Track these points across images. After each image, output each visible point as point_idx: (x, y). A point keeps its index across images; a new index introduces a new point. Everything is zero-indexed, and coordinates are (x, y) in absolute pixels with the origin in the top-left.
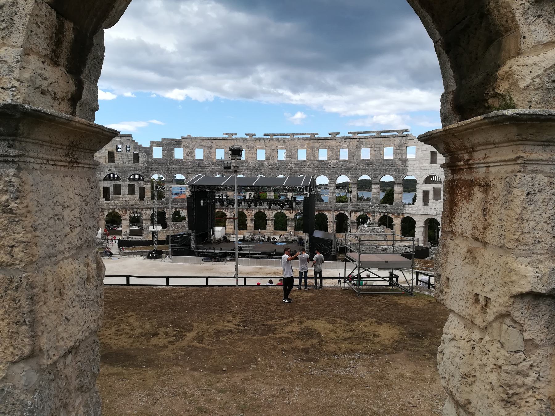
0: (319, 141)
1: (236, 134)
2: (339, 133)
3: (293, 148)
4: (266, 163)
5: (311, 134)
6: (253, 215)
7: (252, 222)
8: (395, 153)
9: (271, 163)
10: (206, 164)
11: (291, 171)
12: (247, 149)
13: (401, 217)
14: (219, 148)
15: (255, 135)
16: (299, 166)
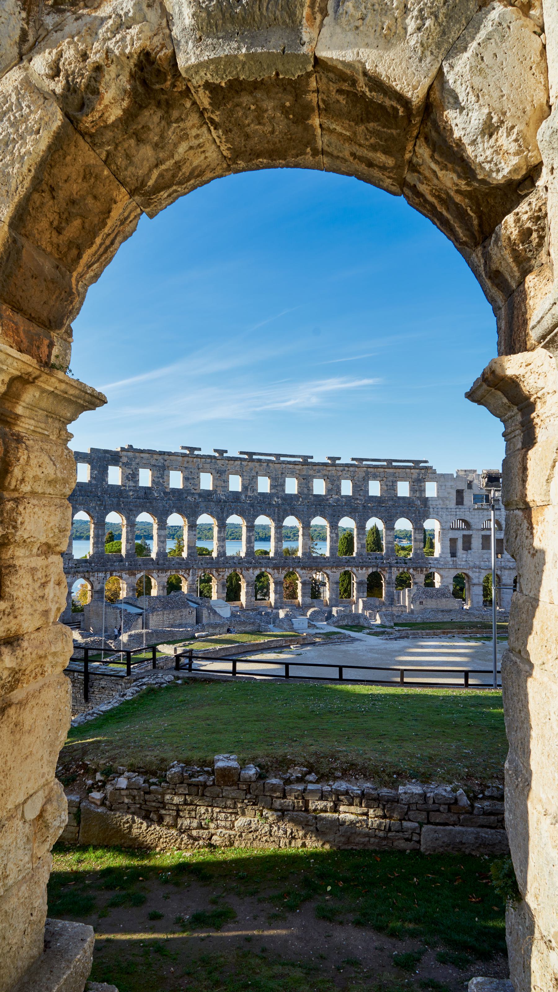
0: (314, 468)
1: (200, 449)
2: (339, 459)
3: (280, 476)
4: (243, 497)
5: (305, 456)
6: (226, 578)
7: (224, 589)
8: (412, 490)
9: (250, 497)
10: (156, 495)
11: (279, 510)
12: (216, 475)
13: (425, 572)
14: (176, 469)
15: (226, 452)
16: (288, 501)
